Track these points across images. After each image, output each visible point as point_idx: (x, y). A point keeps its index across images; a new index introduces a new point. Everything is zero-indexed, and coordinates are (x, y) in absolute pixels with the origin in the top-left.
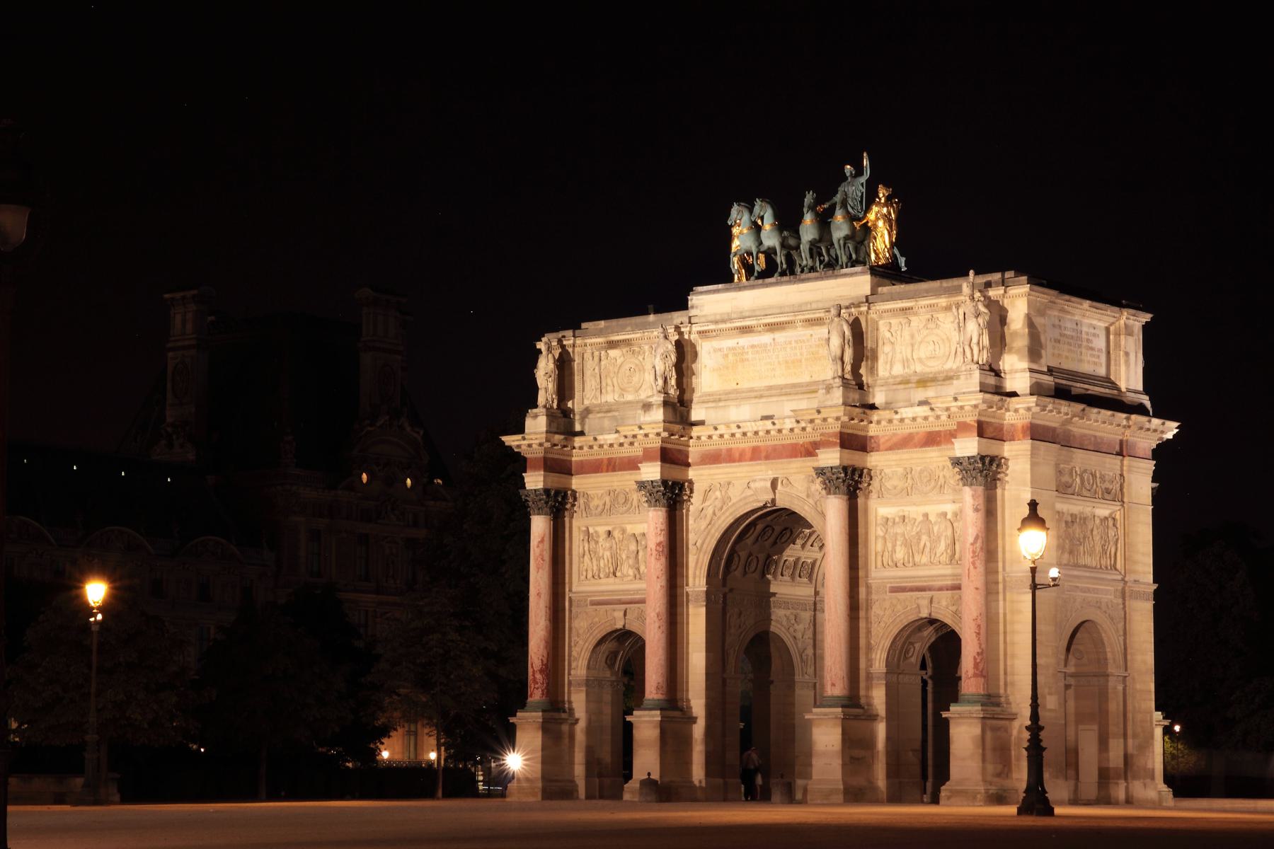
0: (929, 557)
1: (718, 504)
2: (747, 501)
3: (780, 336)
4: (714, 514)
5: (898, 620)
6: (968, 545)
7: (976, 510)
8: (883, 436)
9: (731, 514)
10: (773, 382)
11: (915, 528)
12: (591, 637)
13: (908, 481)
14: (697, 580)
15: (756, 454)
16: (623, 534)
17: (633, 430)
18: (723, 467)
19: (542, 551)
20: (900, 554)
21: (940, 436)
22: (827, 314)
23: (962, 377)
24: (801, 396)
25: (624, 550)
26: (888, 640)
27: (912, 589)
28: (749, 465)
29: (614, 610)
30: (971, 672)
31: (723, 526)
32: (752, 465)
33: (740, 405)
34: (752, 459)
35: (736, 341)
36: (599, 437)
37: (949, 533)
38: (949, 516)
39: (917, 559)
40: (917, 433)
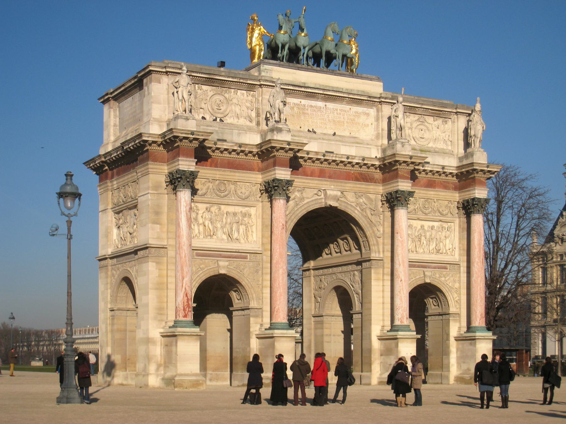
2: (317, 202)
3: (330, 105)
5: (412, 283)
6: (482, 246)
9: (305, 209)
10: (325, 132)
11: (416, 233)
15: (322, 174)
17: (282, 144)
21: (435, 183)
24: (351, 145)
25: (219, 221)
27: (419, 267)
29: (221, 261)
31: (299, 215)
33: (311, 142)
34: (319, 177)
35: (300, 100)
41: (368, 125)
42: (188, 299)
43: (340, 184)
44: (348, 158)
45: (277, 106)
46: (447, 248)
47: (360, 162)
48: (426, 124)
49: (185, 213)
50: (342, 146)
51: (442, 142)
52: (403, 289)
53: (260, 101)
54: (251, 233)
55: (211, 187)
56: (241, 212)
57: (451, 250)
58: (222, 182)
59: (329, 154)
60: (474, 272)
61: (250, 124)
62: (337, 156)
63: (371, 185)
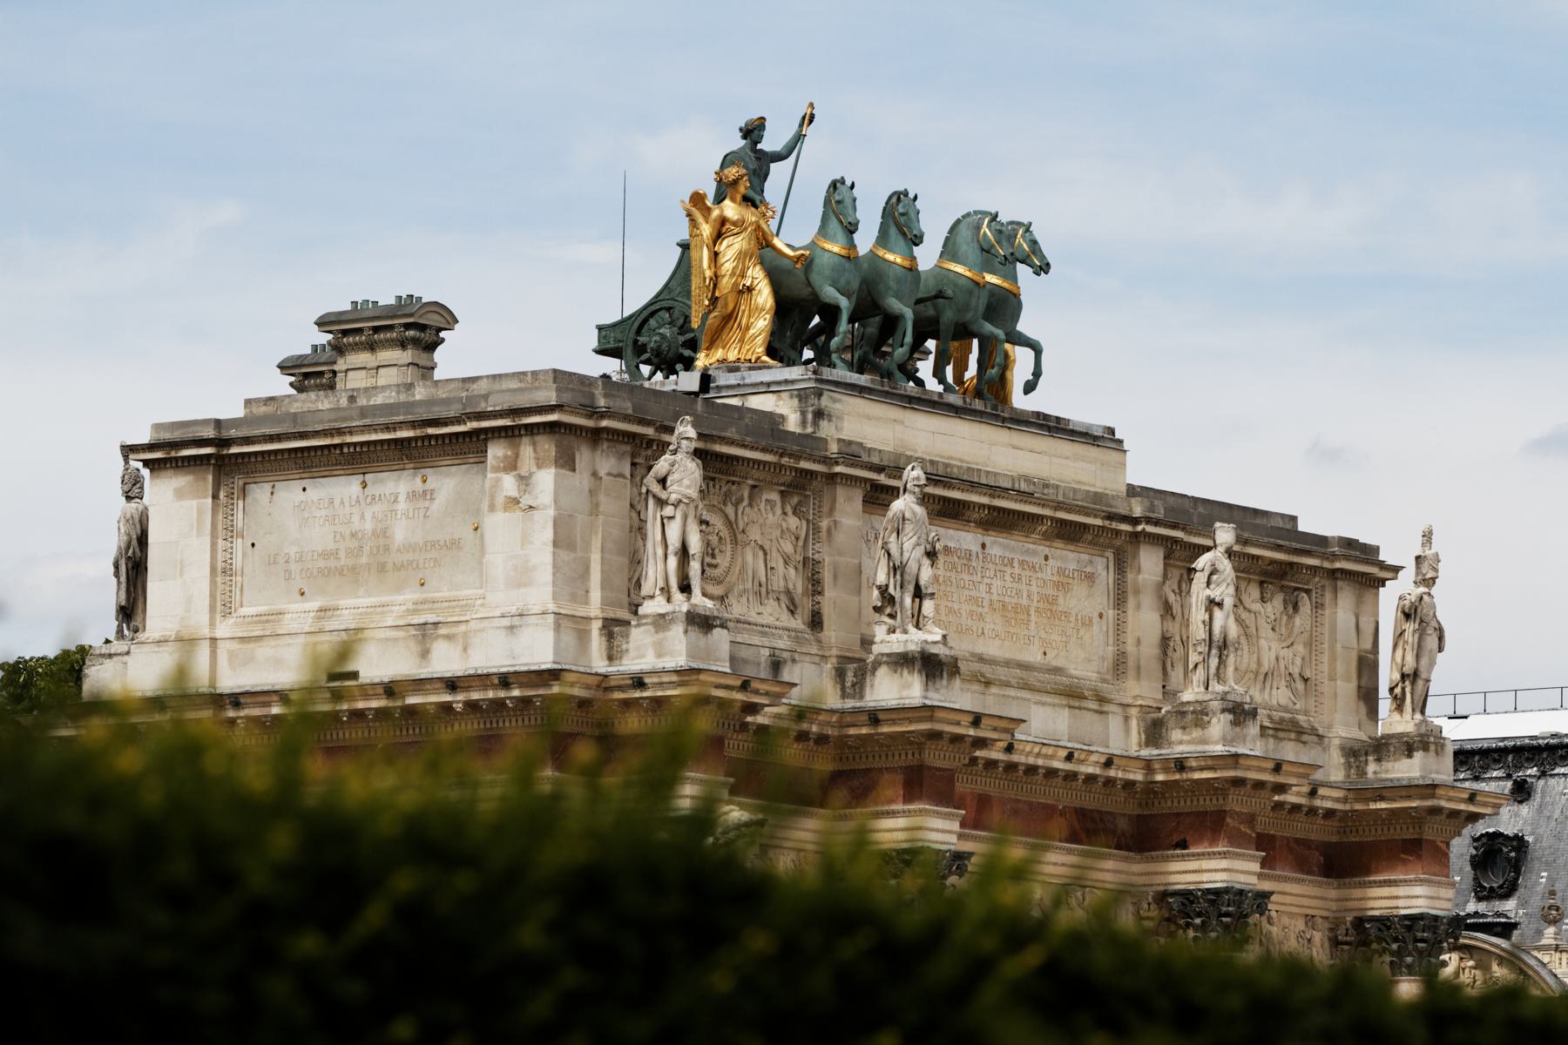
3: (999, 545)
17: (958, 723)
22: (1107, 523)
23: (1432, 747)
24: (1056, 700)
45: (912, 567)
47: (1098, 771)
50: (1034, 707)
53: (824, 534)
62: (1044, 750)
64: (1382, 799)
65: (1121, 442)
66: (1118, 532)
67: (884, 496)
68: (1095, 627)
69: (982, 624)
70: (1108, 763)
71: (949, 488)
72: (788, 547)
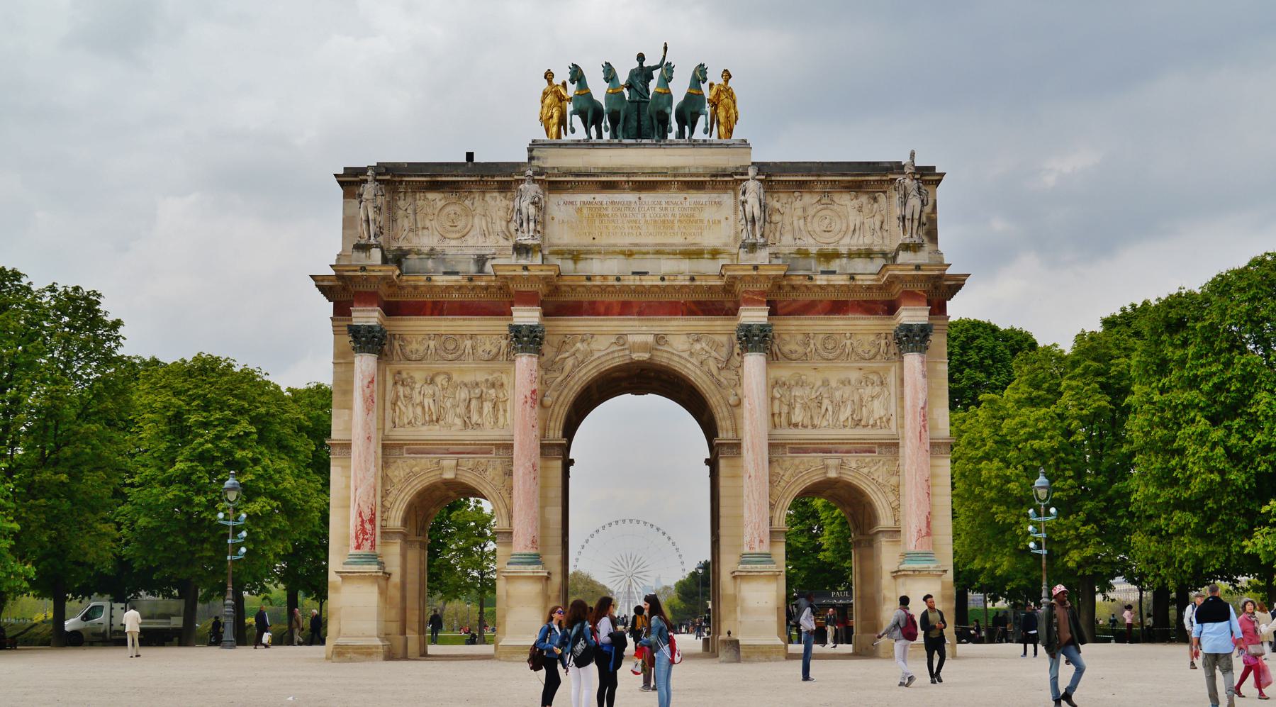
0: (831, 419)
1: (580, 357)
2: (616, 355)
3: (648, 197)
4: (574, 366)
5: (801, 480)
6: (919, 409)
7: (924, 376)
8: (781, 302)
10: (637, 241)
11: (814, 392)
12: (409, 487)
13: (812, 346)
14: (551, 433)
15: (625, 309)
16: (448, 381)
17: (515, 271)
18: (590, 320)
19: (372, 392)
20: (798, 417)
22: (713, 179)
26: (788, 500)
27: (815, 451)
28: (618, 320)
30: (924, 532)
32: (623, 320)
33: (605, 259)
34: (620, 315)
35: (593, 196)
36: (433, 278)
37: (856, 398)
38: (853, 382)
39: (815, 422)
40: (821, 301)
41: (719, 221)
42: (363, 522)
43: (658, 323)
44: (663, 279)
45: (524, 211)
46: (876, 416)
47: (687, 283)
48: (835, 207)
49: (361, 389)
50: (662, 261)
51: (868, 235)
52: (752, 491)
54: (501, 412)
55: (432, 346)
56: (487, 380)
57: (884, 419)
58: (449, 337)
59: (626, 278)
60: (907, 456)
61: (506, 243)
62: (643, 277)
63: (717, 320)
64: (883, 276)
65: (744, 144)
66: (726, 182)
67: (560, 186)
68: (723, 223)
69: (639, 230)
70: (692, 279)
71: (598, 176)
72: (502, 213)
